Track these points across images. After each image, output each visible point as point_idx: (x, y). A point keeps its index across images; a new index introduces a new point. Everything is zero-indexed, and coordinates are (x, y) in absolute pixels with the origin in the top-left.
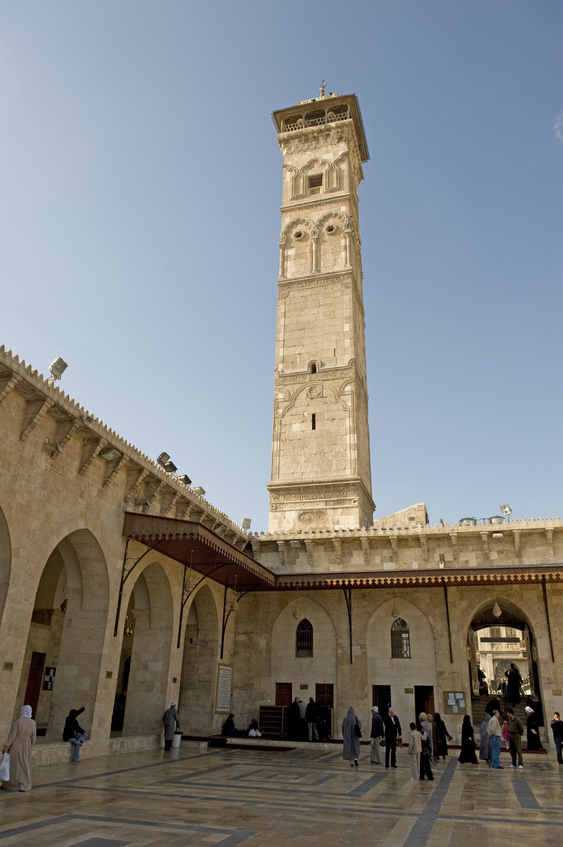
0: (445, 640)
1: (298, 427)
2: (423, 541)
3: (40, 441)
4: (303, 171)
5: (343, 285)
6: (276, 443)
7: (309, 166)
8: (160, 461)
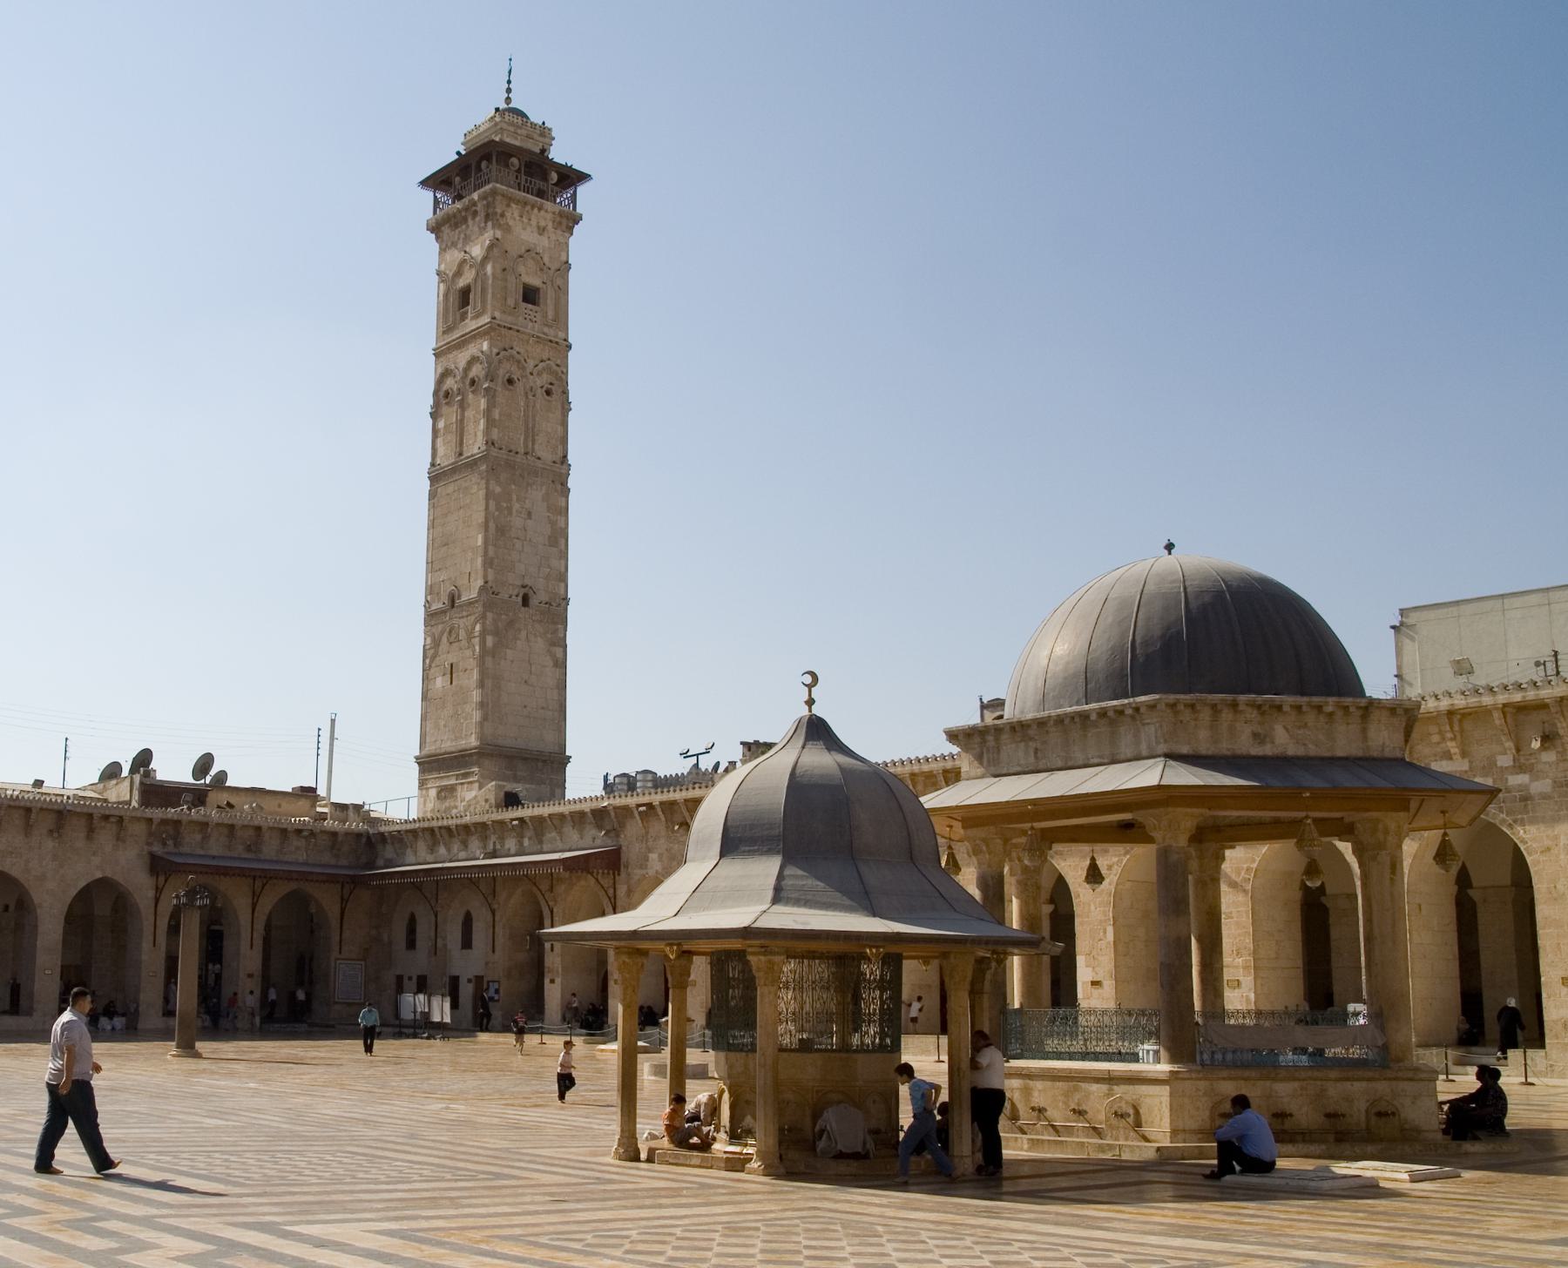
1: (440, 682)
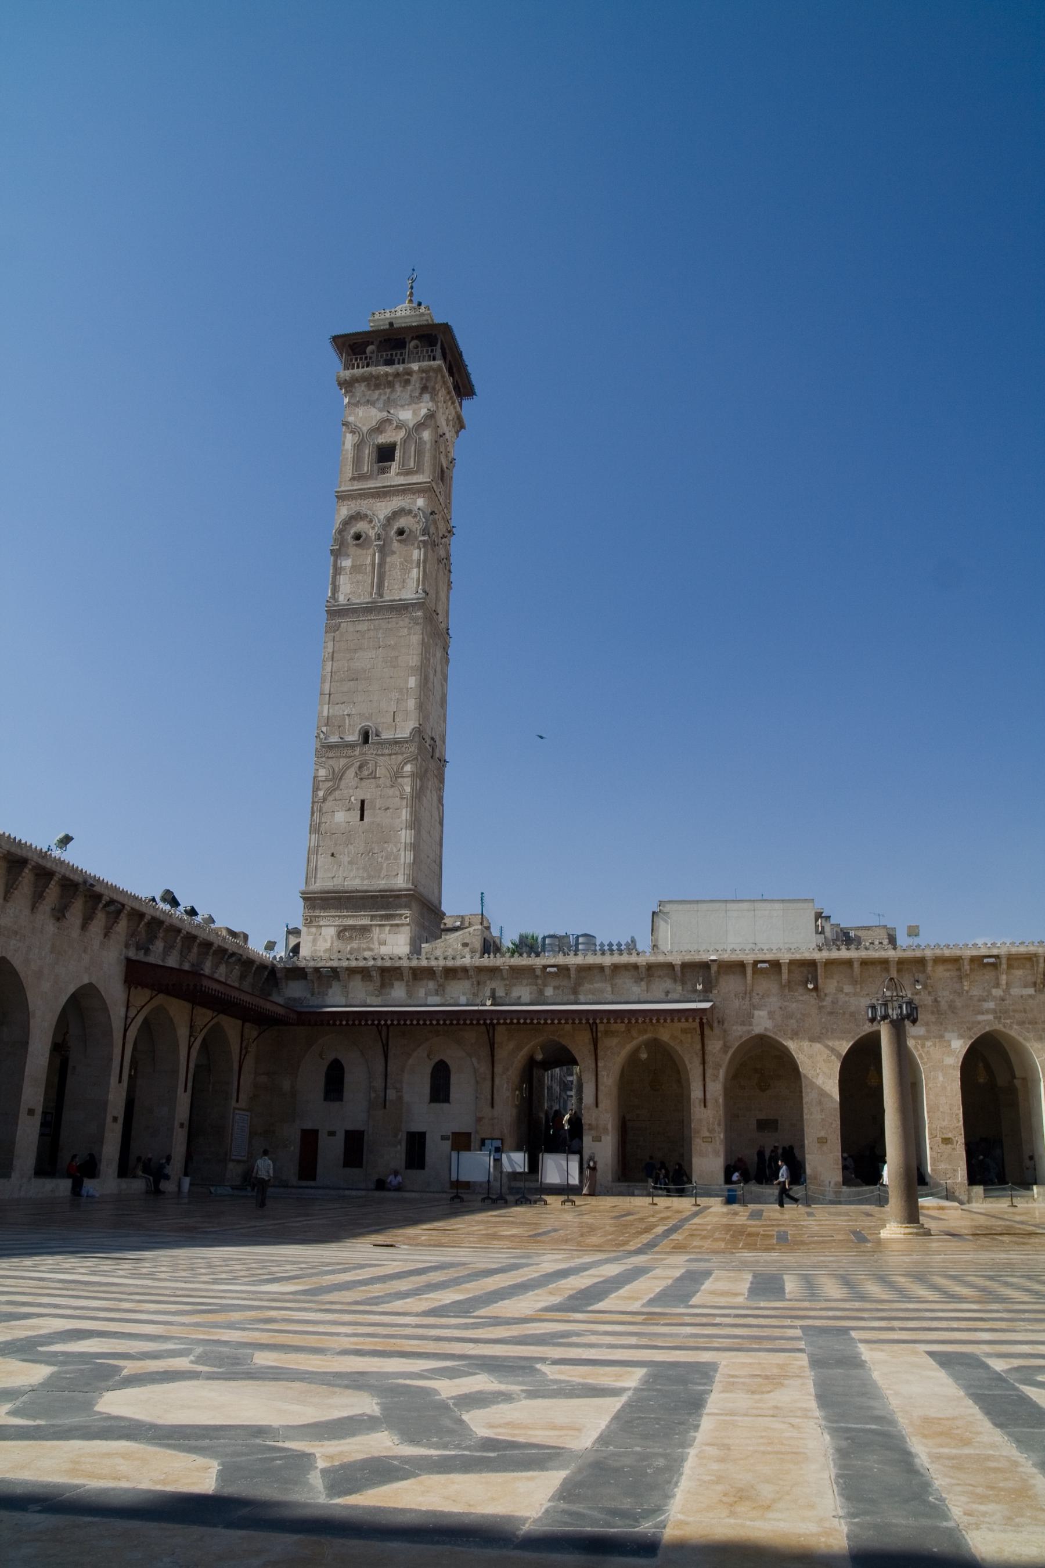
0: (489, 1083)
1: (342, 817)
2: (471, 973)
3: (48, 909)
4: (370, 436)
5: (412, 619)
6: (313, 836)
7: (378, 428)
8: (164, 899)
